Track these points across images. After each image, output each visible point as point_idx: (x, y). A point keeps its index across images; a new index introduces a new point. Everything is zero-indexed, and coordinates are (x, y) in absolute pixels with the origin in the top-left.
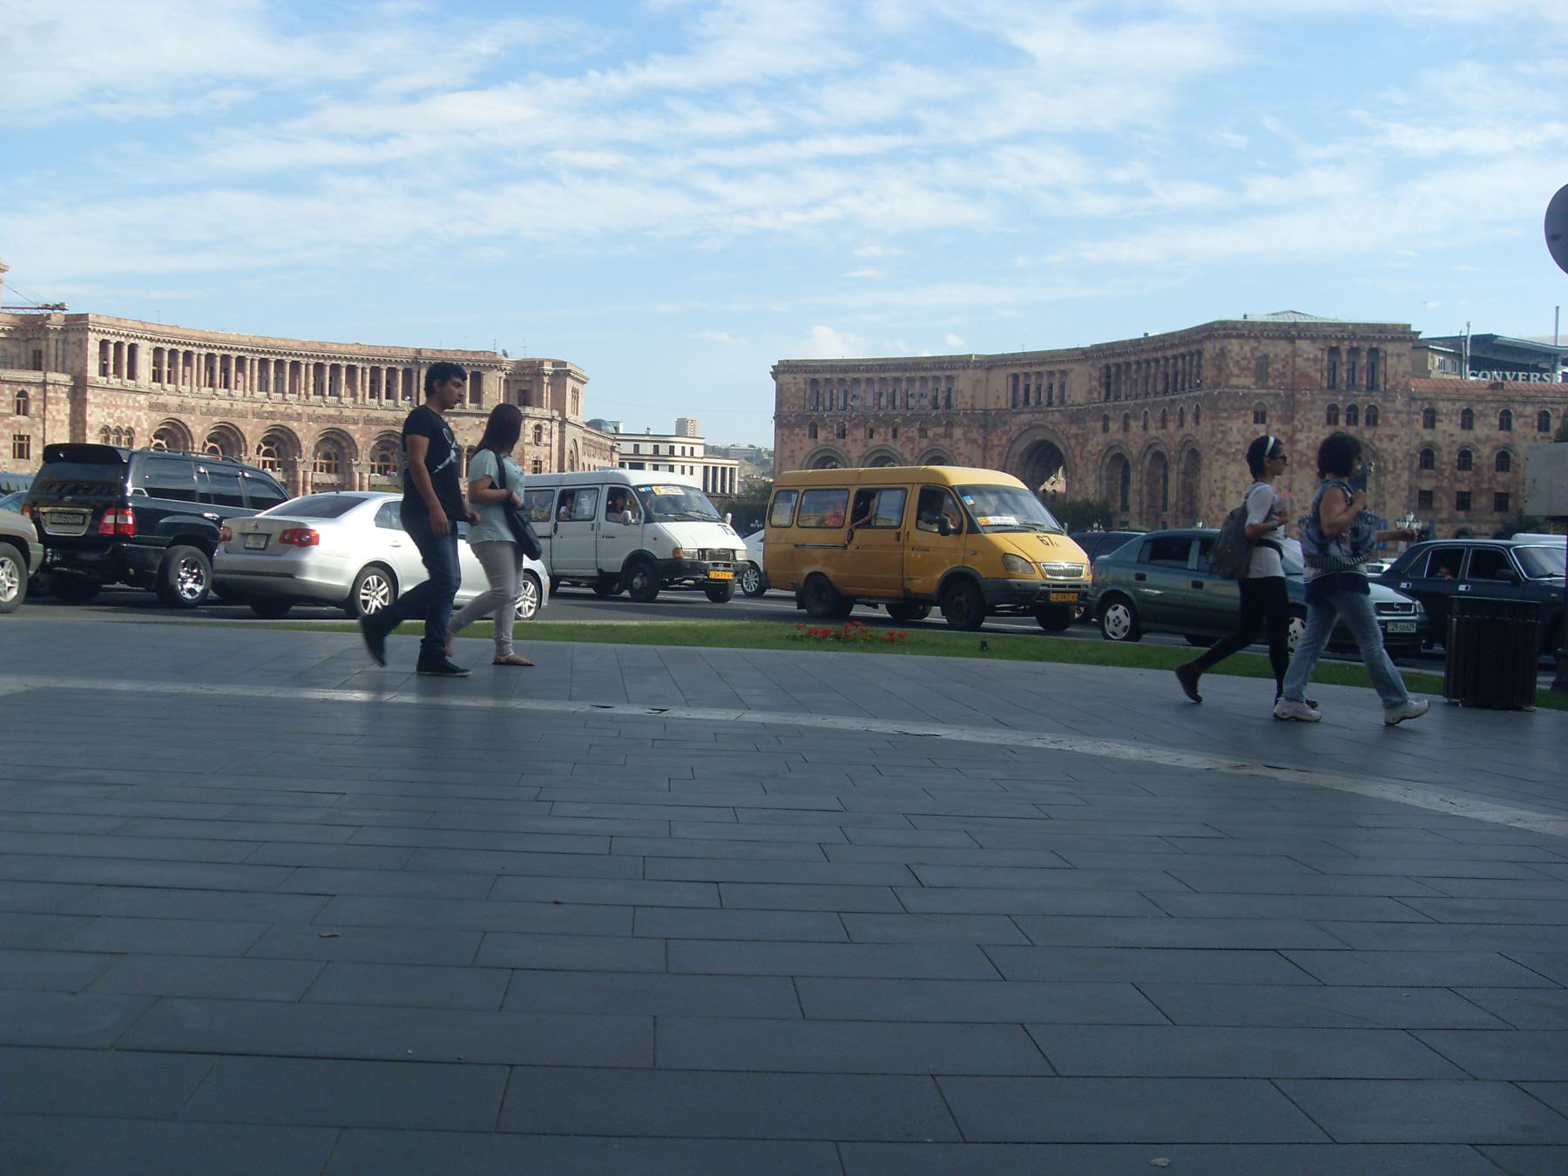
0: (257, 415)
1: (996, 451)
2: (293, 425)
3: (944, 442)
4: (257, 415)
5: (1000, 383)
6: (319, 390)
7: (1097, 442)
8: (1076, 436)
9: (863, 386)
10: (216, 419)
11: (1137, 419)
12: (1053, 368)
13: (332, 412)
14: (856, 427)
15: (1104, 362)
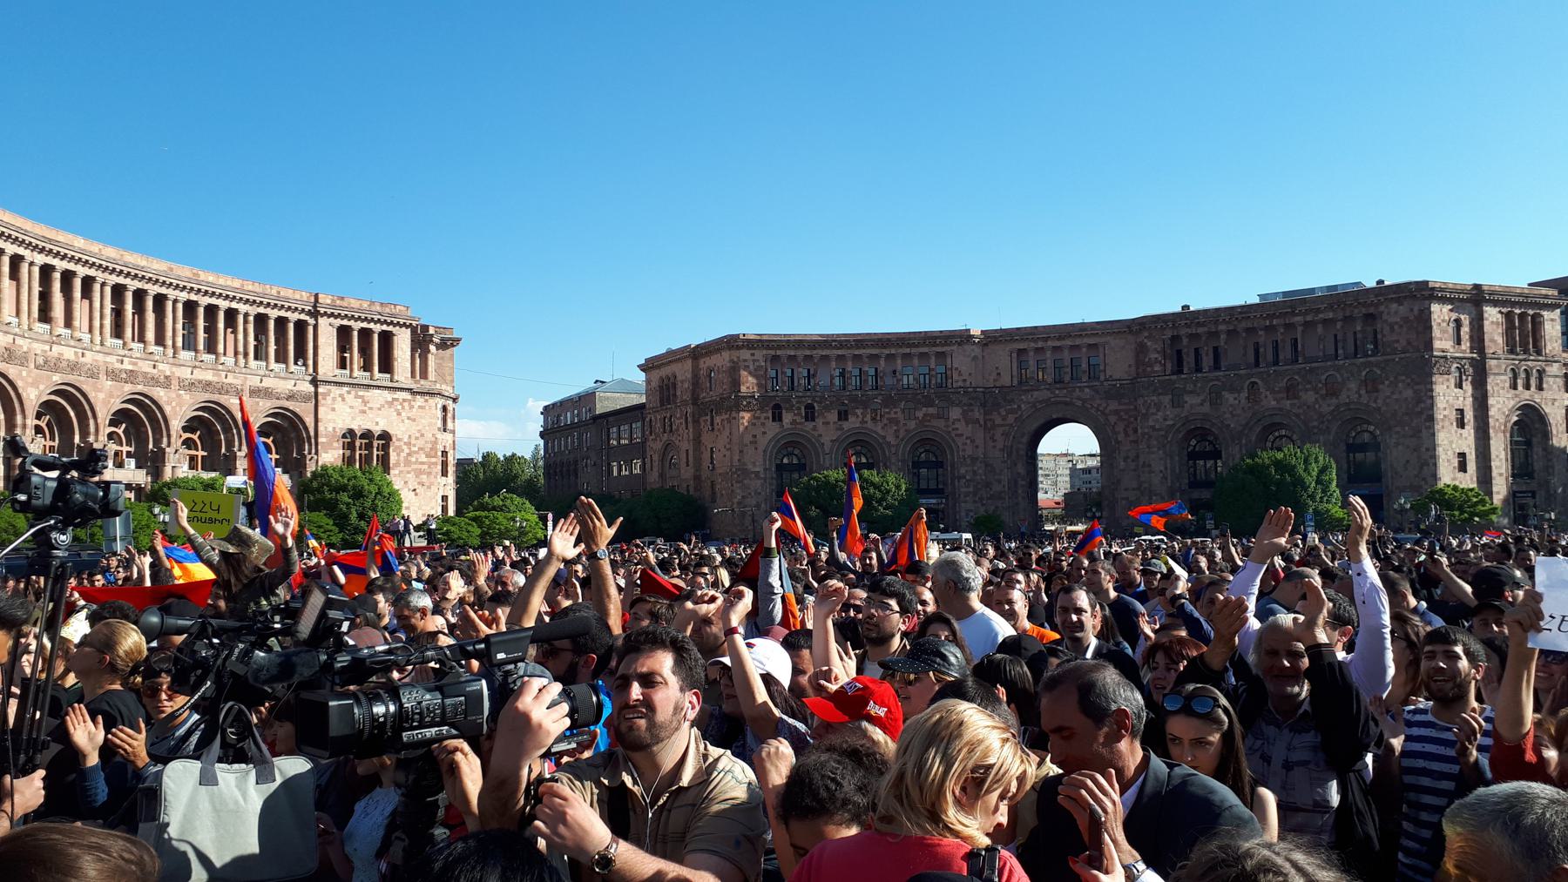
0: (113, 375)
1: (1000, 431)
2: (160, 394)
3: (940, 423)
4: (113, 375)
5: (1002, 359)
6: (189, 344)
7: (1163, 415)
8: (1116, 412)
9: (833, 364)
10: (57, 378)
11: (1232, 390)
12: (1078, 342)
13: (208, 376)
14: (828, 408)
15: (1169, 334)
